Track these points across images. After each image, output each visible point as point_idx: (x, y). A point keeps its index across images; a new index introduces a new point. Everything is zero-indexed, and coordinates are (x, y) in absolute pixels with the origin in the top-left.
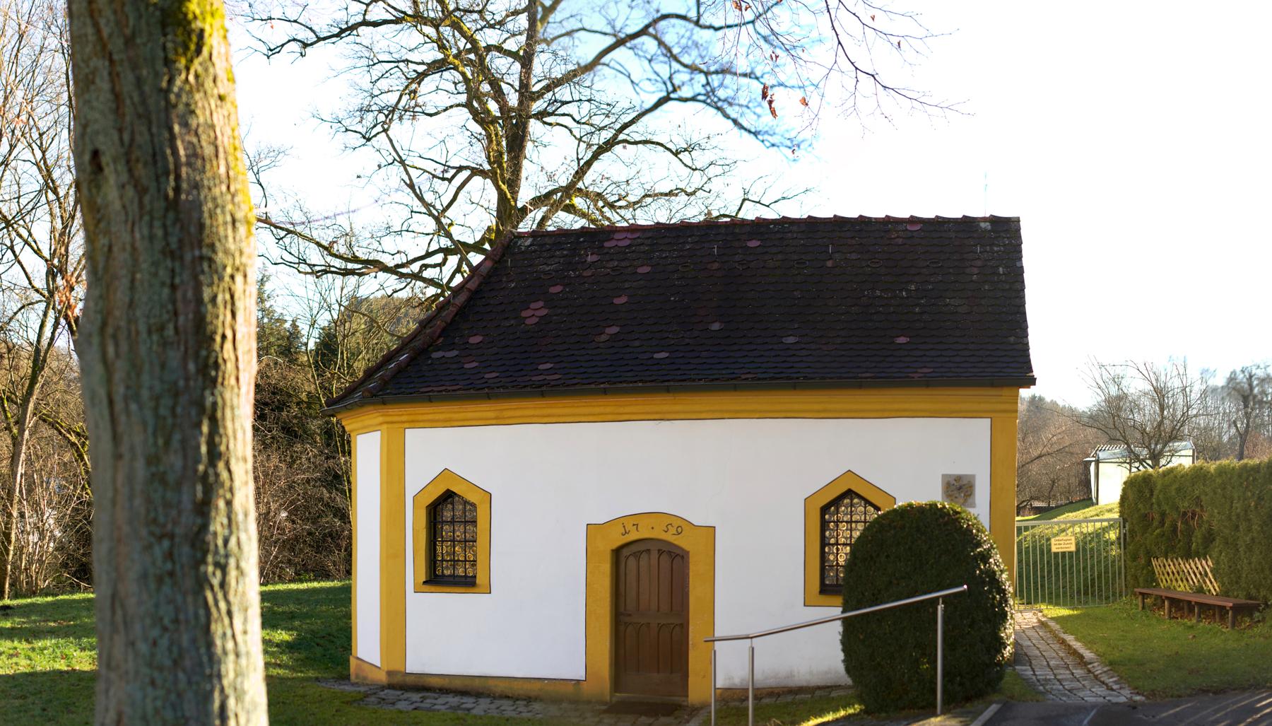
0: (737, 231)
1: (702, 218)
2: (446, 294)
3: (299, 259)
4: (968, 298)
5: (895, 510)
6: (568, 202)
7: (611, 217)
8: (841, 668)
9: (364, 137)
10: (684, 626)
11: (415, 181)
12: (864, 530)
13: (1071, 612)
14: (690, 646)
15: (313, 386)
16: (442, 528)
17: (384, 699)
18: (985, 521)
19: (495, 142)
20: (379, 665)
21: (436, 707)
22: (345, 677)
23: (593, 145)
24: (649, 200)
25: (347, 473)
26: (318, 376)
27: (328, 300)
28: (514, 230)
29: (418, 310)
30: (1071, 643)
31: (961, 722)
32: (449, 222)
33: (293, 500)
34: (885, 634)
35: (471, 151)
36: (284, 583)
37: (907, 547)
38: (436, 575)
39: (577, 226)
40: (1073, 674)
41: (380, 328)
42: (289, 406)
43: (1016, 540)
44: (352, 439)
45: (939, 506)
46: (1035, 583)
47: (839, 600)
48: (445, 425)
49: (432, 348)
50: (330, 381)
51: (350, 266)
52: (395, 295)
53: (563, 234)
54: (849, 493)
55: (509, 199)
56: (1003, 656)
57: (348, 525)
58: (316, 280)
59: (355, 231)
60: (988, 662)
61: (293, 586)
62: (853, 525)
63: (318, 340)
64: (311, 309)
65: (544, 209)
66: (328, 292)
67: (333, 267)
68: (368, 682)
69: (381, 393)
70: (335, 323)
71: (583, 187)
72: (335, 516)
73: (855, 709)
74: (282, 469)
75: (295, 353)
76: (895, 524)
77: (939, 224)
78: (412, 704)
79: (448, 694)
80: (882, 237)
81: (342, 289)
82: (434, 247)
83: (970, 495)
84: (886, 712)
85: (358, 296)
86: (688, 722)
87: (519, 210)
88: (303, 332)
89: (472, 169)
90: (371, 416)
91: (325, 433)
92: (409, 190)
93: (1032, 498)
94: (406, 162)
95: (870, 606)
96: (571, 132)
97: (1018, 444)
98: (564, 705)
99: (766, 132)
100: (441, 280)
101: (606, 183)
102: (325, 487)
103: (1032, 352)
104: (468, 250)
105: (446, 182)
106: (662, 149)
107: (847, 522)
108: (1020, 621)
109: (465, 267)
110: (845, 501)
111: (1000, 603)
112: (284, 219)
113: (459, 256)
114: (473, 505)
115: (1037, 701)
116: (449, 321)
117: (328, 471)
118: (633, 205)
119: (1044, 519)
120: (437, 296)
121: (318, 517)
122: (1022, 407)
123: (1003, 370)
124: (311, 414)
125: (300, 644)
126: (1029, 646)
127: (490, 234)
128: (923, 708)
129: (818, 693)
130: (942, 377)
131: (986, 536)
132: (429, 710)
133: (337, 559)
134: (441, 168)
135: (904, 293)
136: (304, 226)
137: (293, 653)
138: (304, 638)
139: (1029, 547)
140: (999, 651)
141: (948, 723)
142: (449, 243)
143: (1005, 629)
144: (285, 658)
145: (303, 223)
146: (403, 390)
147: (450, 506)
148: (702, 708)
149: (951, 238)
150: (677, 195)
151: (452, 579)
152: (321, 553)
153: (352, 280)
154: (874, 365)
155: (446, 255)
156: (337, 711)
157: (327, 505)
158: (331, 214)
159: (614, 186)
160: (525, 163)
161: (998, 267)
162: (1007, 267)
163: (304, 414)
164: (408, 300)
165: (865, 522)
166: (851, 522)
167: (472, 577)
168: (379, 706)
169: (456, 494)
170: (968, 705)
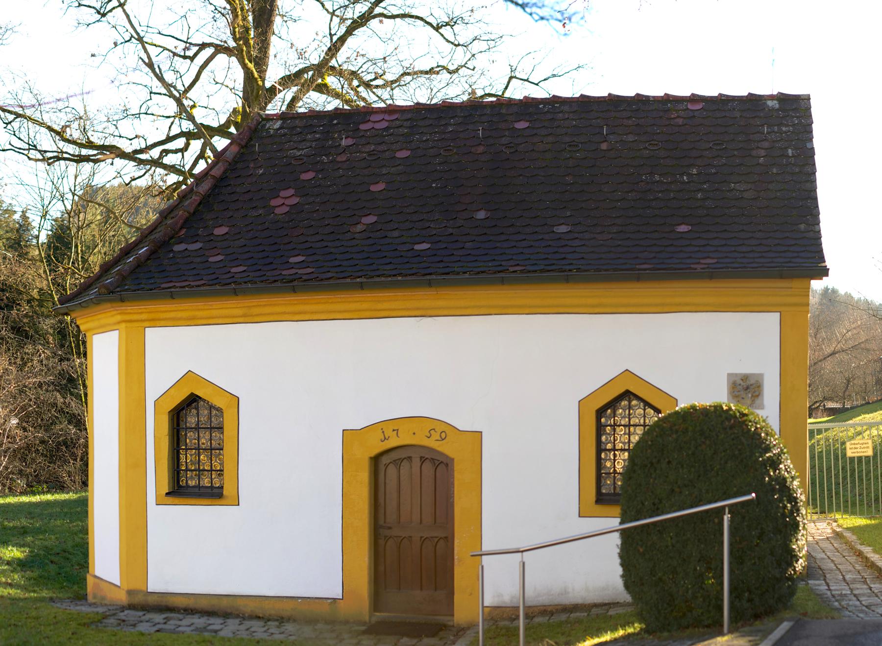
0: (504, 111)
1: (465, 98)
2: (189, 182)
3: (29, 145)
4: (754, 182)
5: (677, 413)
6: (320, 81)
7: (367, 97)
8: (619, 583)
9: (99, 13)
10: (449, 540)
11: (154, 59)
12: (643, 434)
13: (869, 522)
14: (456, 561)
15: (45, 282)
16: (186, 435)
17: (124, 621)
18: (774, 423)
19: (240, 17)
20: (118, 584)
21: (180, 629)
22: (81, 597)
23: (347, 19)
24: (408, 78)
25: (82, 376)
26: (50, 271)
27: (61, 189)
28: (262, 112)
29: (158, 199)
30: (868, 556)
31: (750, 641)
32: (191, 103)
33: (25, 405)
34: (667, 547)
35: (215, 27)
36: (14, 495)
37: (690, 453)
38: (180, 487)
39: (330, 107)
40: (870, 588)
41: (117, 219)
42: (19, 304)
43: (808, 444)
44: (88, 340)
45: (725, 408)
46: (830, 490)
47: (617, 510)
48: (189, 324)
49: (173, 240)
50: (63, 276)
51: (85, 152)
52: (133, 183)
53: (315, 116)
54: (627, 395)
55: (256, 79)
56: (794, 570)
57: (84, 433)
58: (48, 167)
59: (89, 114)
60: (778, 576)
61: (25, 499)
62: (632, 429)
63: (50, 233)
64: (42, 199)
65: (294, 89)
66: (60, 180)
67: (66, 153)
68: (106, 602)
69: (118, 289)
70: (69, 214)
71: (336, 65)
72: (70, 422)
73: (635, 629)
74: (12, 373)
75: (26, 246)
76: (677, 427)
77: (723, 101)
78: (154, 625)
79: (193, 614)
80: (661, 117)
81: (76, 177)
82: (175, 130)
83: (758, 396)
84: (669, 631)
85: (93, 184)
86: (454, 644)
87: (267, 90)
88: (34, 224)
89: (216, 46)
90: (109, 314)
91: (59, 333)
92: (148, 69)
93: (825, 399)
94: (144, 39)
95: (651, 517)
96: (323, 5)
97: (810, 340)
98: (320, 626)
99: (535, 4)
100: (183, 167)
101: (361, 60)
102: (58, 391)
103: (823, 240)
104: (212, 134)
105: (188, 61)
106: (422, 23)
107: (624, 426)
108: (813, 531)
109: (209, 153)
110: (623, 403)
111: (792, 512)
112: (12, 102)
113: (202, 140)
114: (219, 410)
115: (833, 618)
116: (192, 211)
117: (61, 374)
118: (391, 84)
119: (839, 422)
120: (179, 184)
121: (52, 424)
122: (813, 300)
123: (794, 260)
124: (43, 313)
125: (32, 562)
126: (823, 559)
127: (236, 117)
128: (708, 626)
129: (594, 611)
130: (728, 268)
131: (775, 440)
132: (173, 632)
133: (72, 469)
134: (182, 45)
135: (685, 178)
136: (34, 109)
137: (25, 572)
138: (37, 555)
139: (822, 452)
140: (790, 564)
141: (735, 642)
142: (192, 127)
143: (797, 540)
144: (16, 577)
145: (33, 106)
146: (142, 286)
147: (194, 411)
148: (469, 628)
149: (736, 118)
150: (438, 73)
151: (197, 490)
152: (55, 463)
153: (87, 167)
154: (653, 255)
155: (188, 140)
156: (73, 634)
157: (61, 411)
158: (64, 96)
159: (370, 63)
160: (274, 40)
161: (786, 148)
162: (796, 149)
163: (36, 313)
164: (148, 188)
165: (644, 425)
166: (629, 425)
167: (218, 487)
168: (119, 628)
169: (200, 398)
170: (757, 623)
